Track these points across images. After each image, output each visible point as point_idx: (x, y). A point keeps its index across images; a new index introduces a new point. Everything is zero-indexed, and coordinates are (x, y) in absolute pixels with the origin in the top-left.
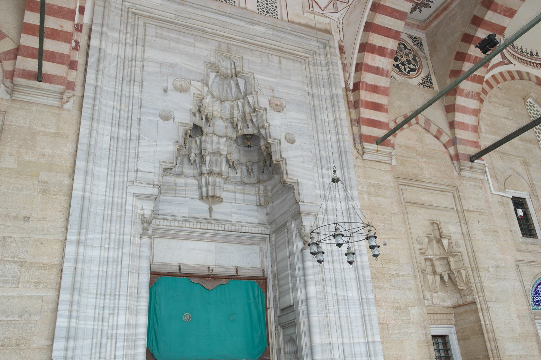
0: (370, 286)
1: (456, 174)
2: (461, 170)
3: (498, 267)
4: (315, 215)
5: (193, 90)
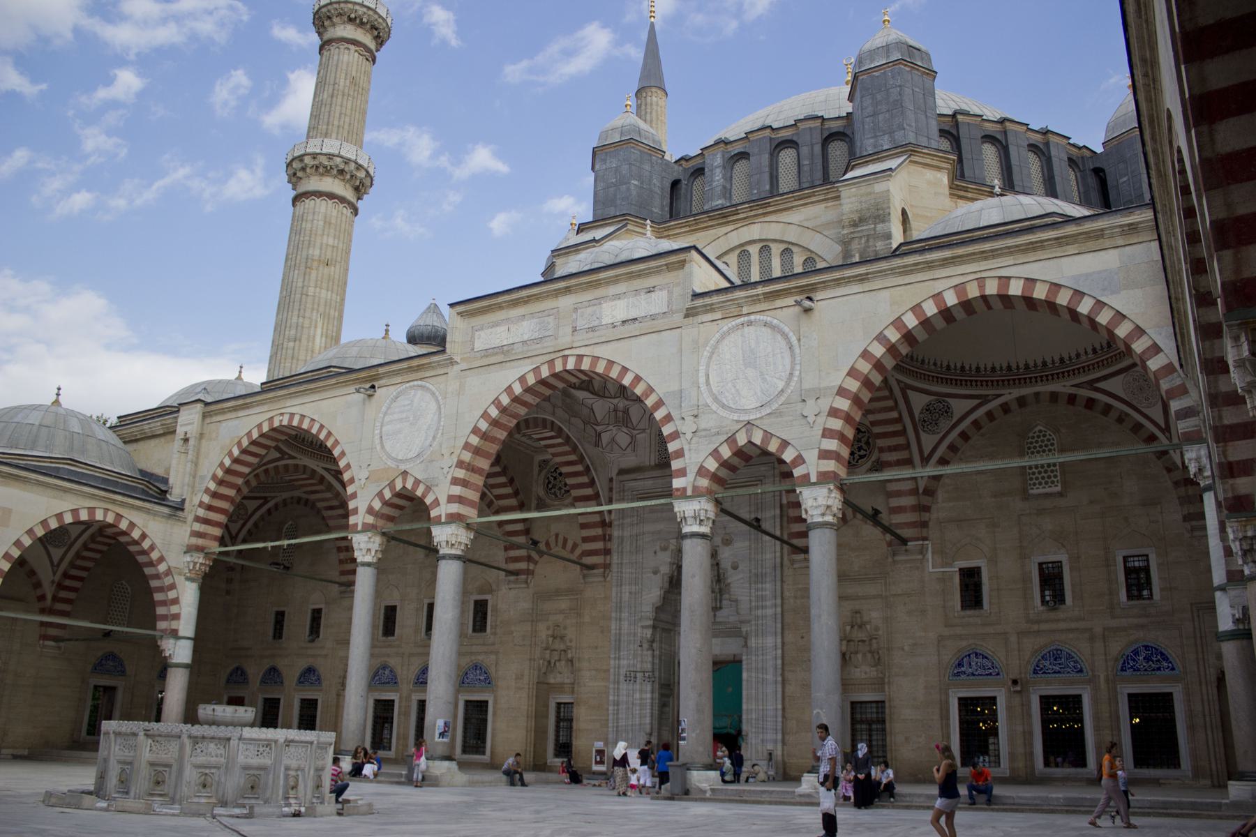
0: (779, 671)
1: (890, 560)
2: (894, 555)
3: (915, 644)
4: (749, 621)
5: (672, 547)
